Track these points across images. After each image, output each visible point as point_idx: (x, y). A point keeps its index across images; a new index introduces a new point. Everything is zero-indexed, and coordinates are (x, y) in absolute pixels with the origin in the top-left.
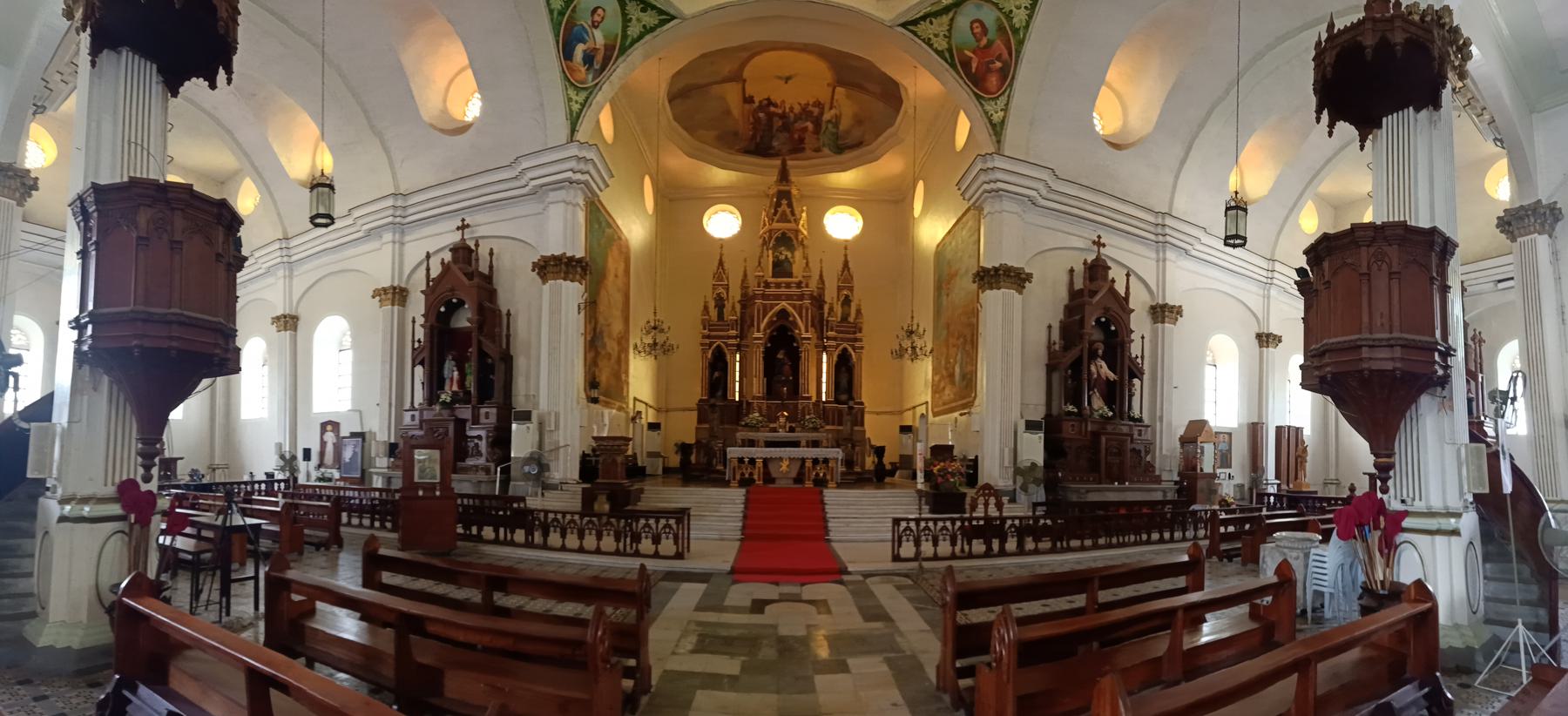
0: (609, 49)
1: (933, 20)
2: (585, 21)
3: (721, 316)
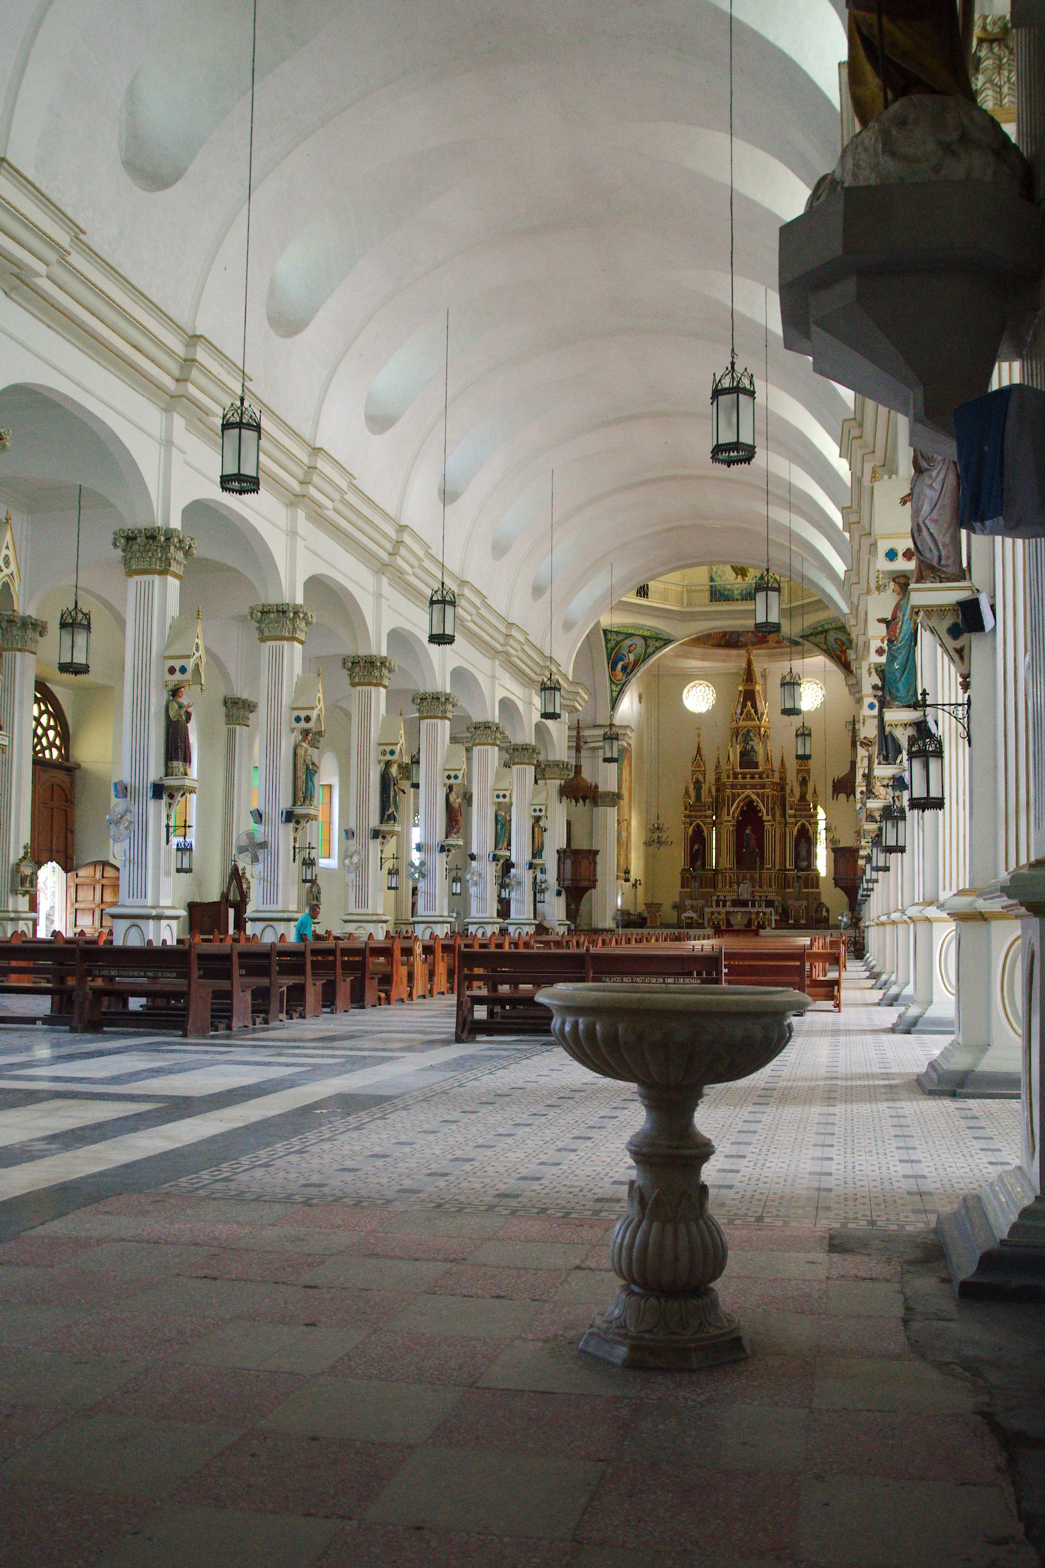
2: (624, 651)
3: (698, 798)
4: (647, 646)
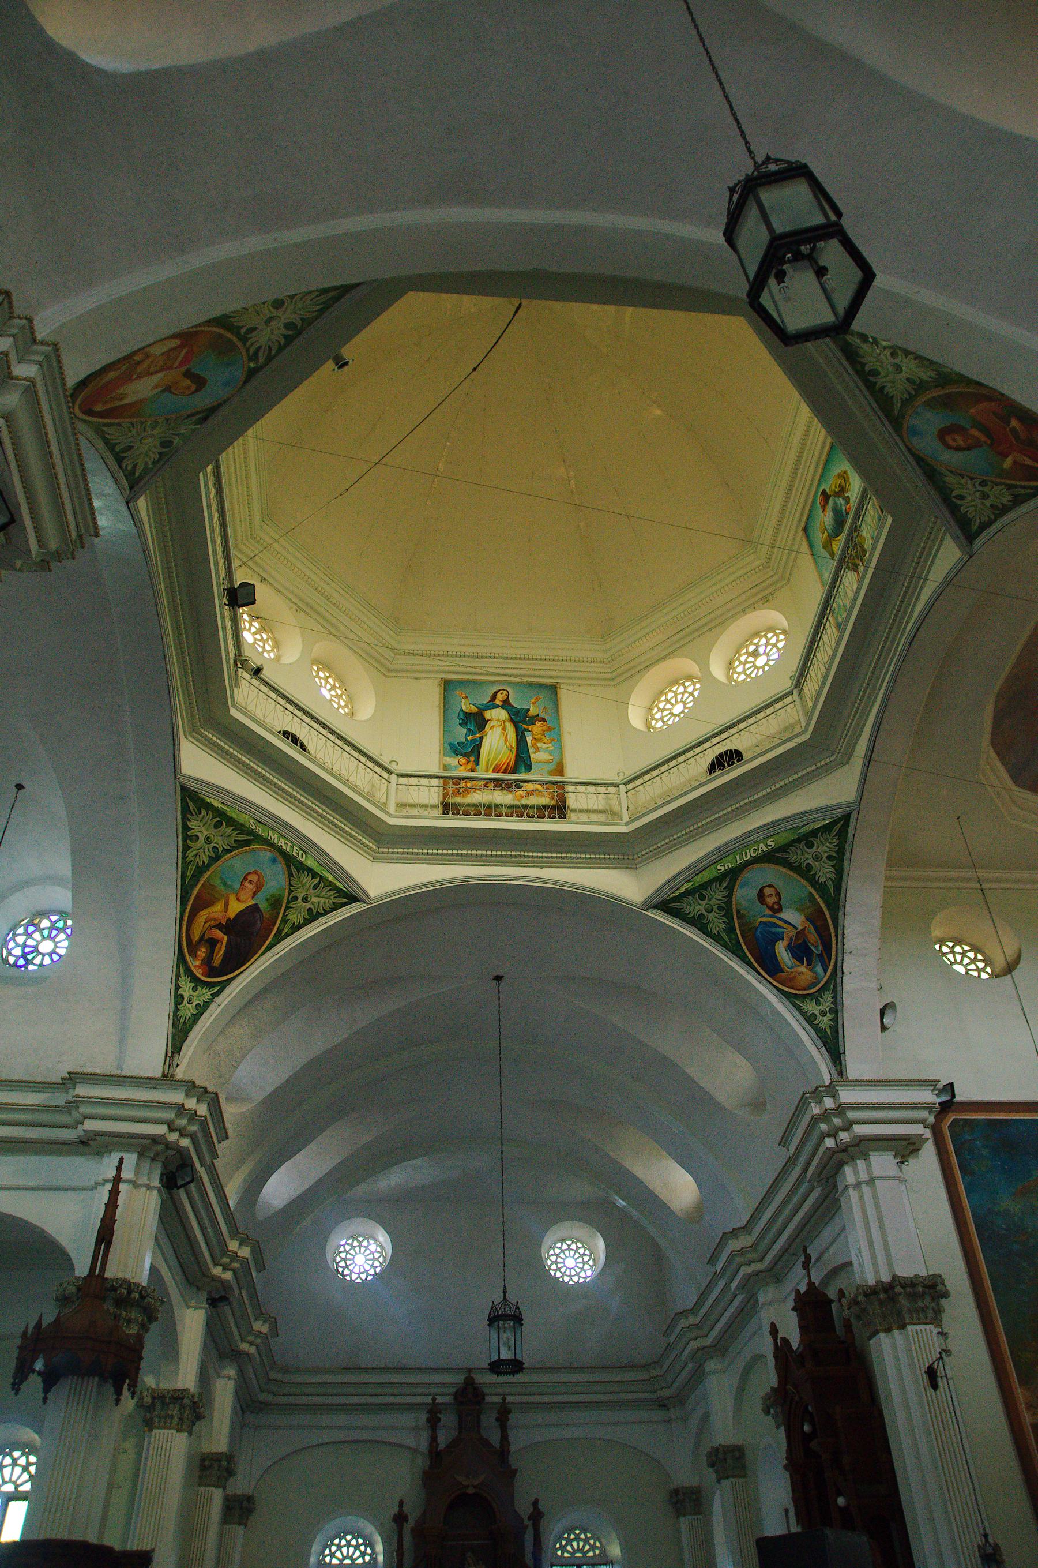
0: (816, 918)
1: (954, 493)
2: (761, 916)
4: (806, 873)
